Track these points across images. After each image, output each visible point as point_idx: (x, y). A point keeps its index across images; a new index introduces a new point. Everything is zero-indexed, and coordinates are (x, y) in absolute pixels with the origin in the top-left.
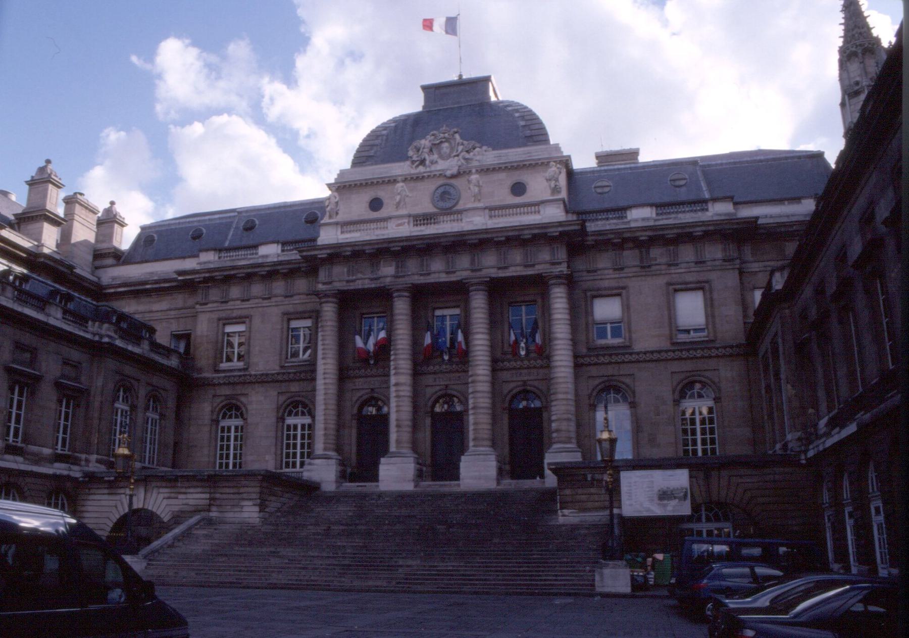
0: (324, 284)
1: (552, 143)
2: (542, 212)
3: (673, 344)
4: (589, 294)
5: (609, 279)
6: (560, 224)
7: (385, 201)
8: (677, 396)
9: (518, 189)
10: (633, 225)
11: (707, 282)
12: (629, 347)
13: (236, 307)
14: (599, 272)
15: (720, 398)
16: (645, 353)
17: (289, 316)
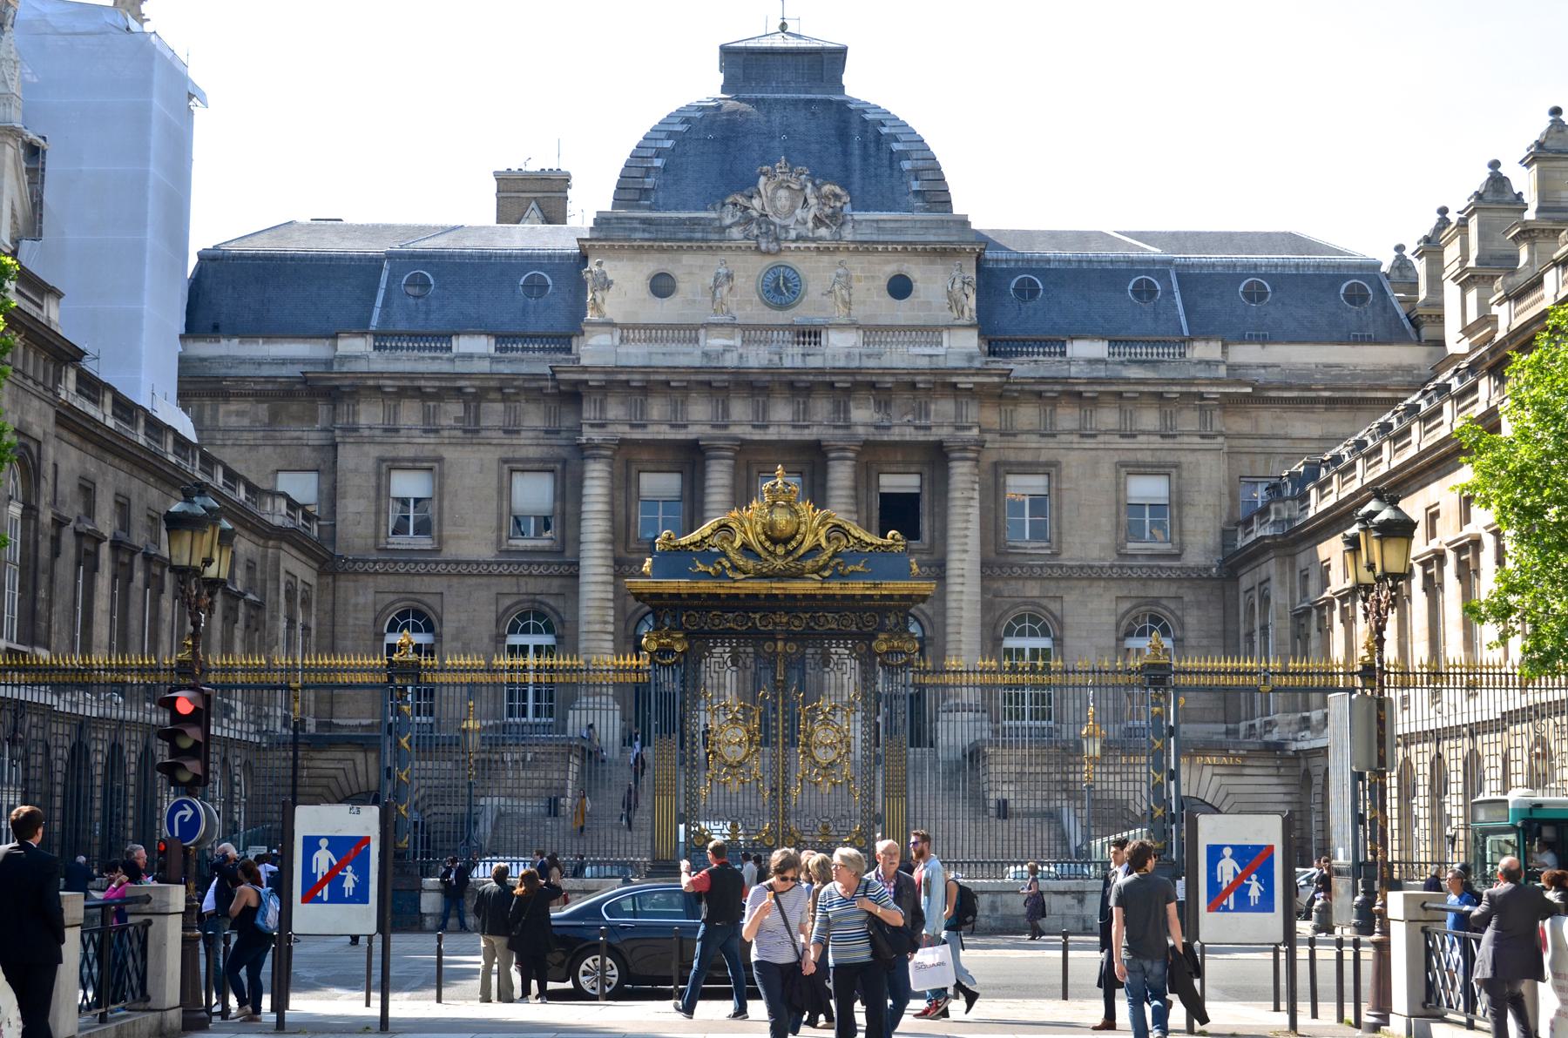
0: (592, 425)
1: (955, 212)
2: (945, 344)
3: (1120, 555)
4: (1001, 470)
5: (1031, 447)
6: (979, 372)
7: (680, 285)
8: (1121, 635)
9: (900, 287)
10: (1074, 371)
11: (1177, 466)
12: (1055, 555)
13: (415, 444)
14: (1020, 438)
15: (1182, 640)
16: (1081, 568)
17: (515, 466)
